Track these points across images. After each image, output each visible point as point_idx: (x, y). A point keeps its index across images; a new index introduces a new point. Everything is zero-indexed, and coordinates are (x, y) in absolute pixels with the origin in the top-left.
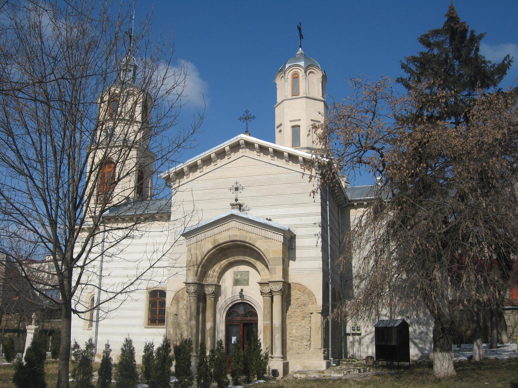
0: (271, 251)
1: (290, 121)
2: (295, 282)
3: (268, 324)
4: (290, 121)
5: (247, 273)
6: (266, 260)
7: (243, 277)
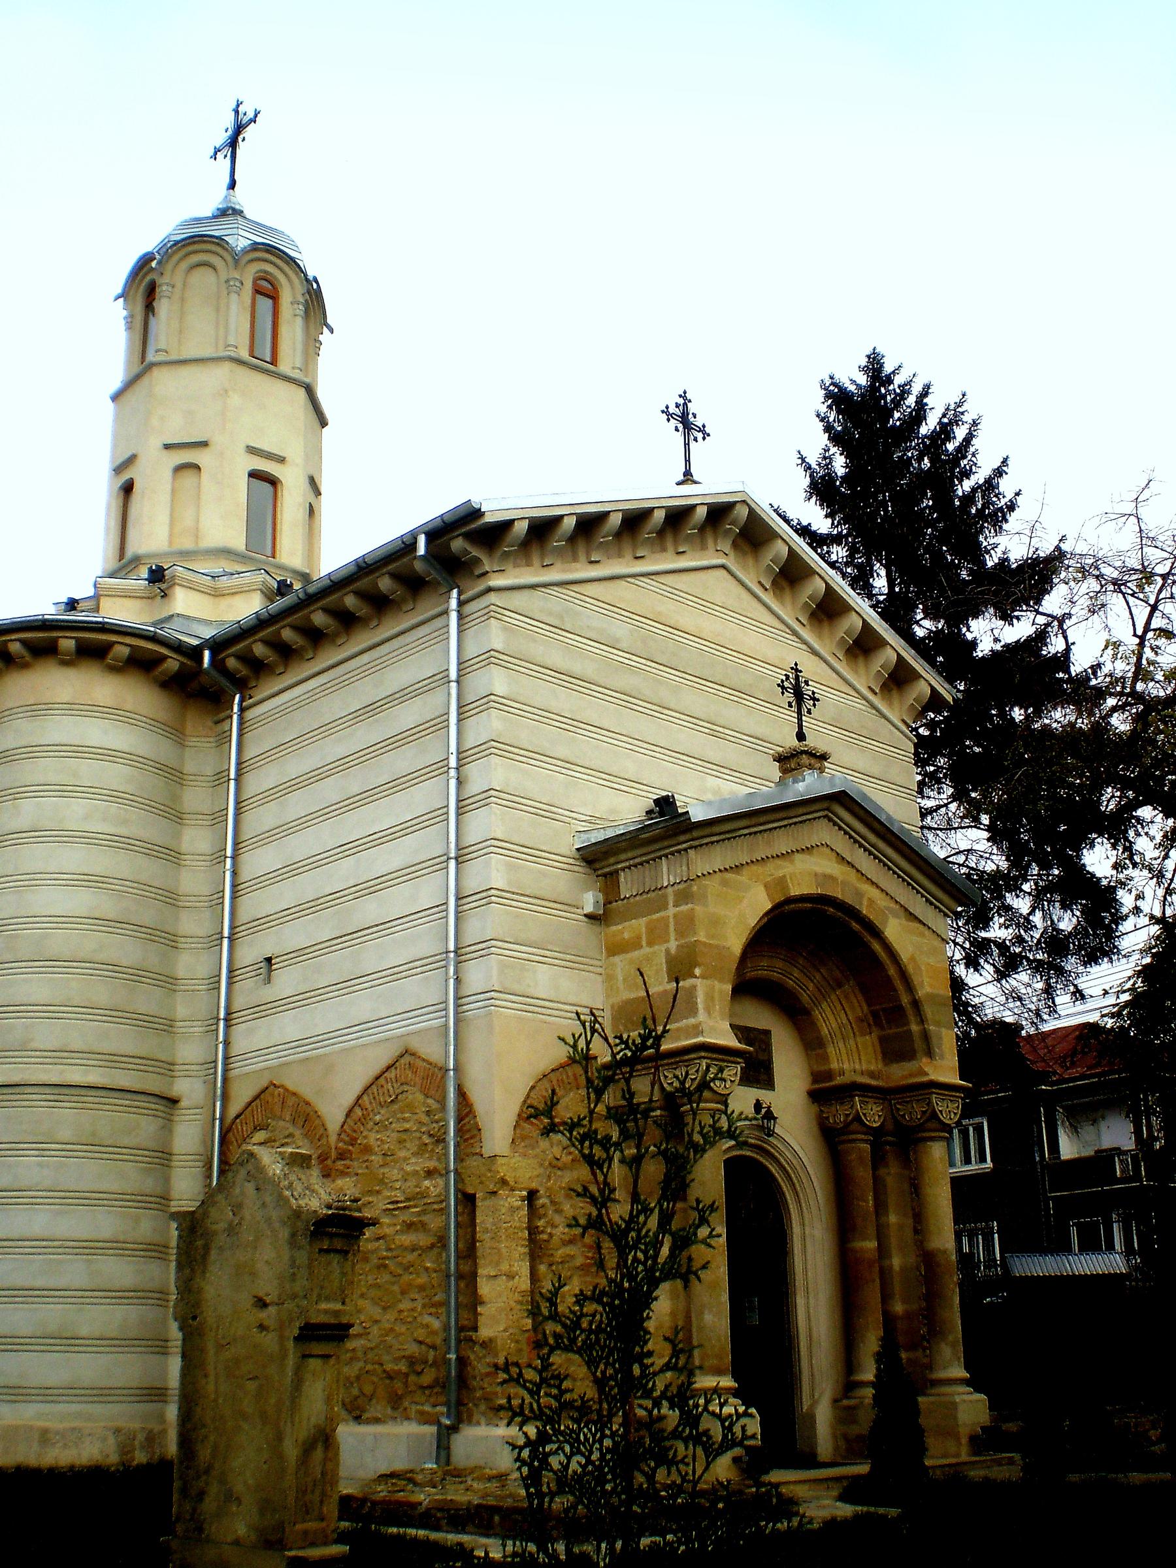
1: (252, 451)
4: (252, 451)
5: (762, 1036)
6: (905, 1000)
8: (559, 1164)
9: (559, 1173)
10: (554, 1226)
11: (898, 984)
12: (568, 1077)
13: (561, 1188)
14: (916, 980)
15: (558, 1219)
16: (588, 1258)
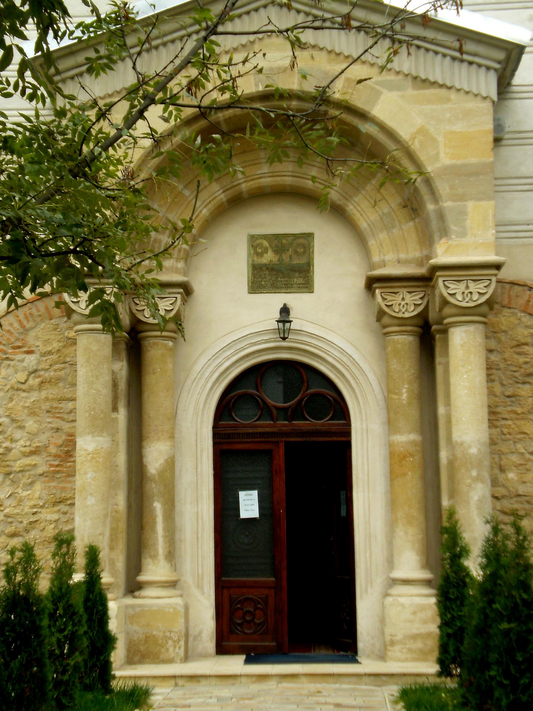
0: (440, 139)
2: (511, 278)
3: (413, 443)
5: (302, 241)
7: (286, 257)
8: (24, 387)
9: (24, 394)
10: (12, 441)
11: (406, 163)
12: (38, 311)
13: (24, 407)
14: (422, 157)
15: (18, 434)
16: (52, 466)
